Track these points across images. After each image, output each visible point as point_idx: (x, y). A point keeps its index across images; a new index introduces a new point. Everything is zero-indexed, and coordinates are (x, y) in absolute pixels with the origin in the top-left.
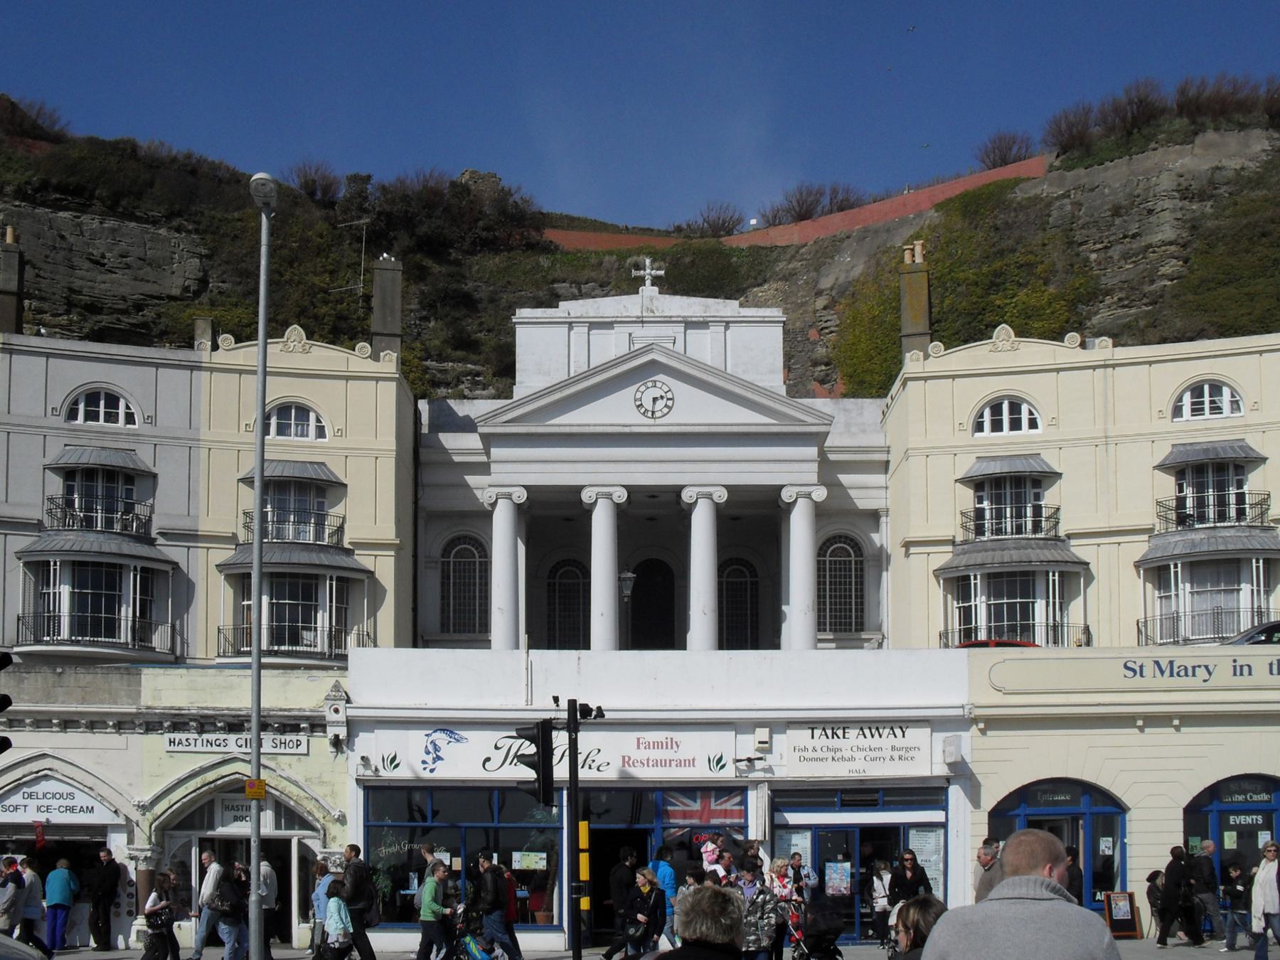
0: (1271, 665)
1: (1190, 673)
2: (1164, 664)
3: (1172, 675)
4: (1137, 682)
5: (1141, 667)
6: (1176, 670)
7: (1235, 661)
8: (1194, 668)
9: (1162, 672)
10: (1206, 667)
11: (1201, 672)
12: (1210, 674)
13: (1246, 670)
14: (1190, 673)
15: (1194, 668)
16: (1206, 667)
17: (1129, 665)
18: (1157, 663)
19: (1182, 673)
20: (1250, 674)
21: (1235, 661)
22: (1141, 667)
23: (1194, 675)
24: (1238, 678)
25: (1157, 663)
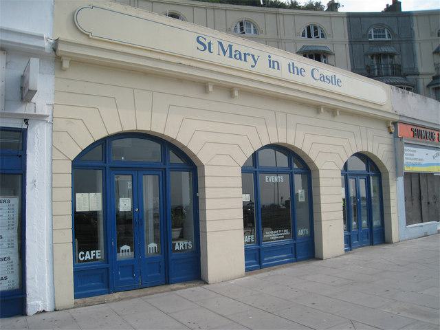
0: (289, 65)
1: (243, 58)
2: (226, 46)
3: (231, 56)
4: (205, 55)
5: (210, 44)
6: (233, 53)
7: (270, 57)
8: (245, 54)
9: (225, 53)
10: (253, 56)
11: (249, 58)
12: (256, 63)
13: (276, 64)
14: (243, 58)
15: (245, 54)
16: (253, 56)
17: (201, 39)
18: (220, 44)
19: (238, 56)
20: (278, 69)
21: (270, 57)
22: (210, 44)
23: (245, 60)
24: (271, 69)
25: (220, 44)
